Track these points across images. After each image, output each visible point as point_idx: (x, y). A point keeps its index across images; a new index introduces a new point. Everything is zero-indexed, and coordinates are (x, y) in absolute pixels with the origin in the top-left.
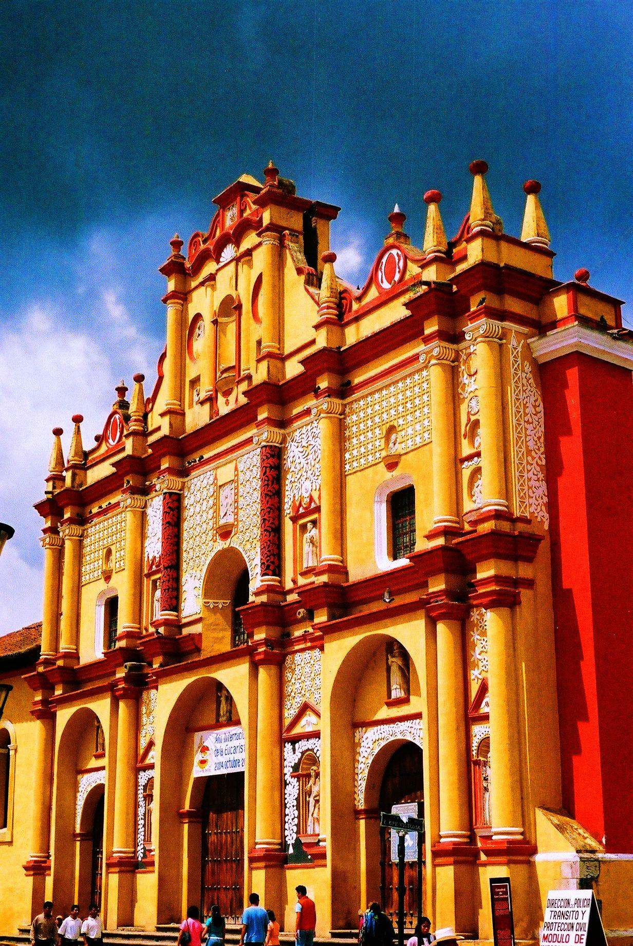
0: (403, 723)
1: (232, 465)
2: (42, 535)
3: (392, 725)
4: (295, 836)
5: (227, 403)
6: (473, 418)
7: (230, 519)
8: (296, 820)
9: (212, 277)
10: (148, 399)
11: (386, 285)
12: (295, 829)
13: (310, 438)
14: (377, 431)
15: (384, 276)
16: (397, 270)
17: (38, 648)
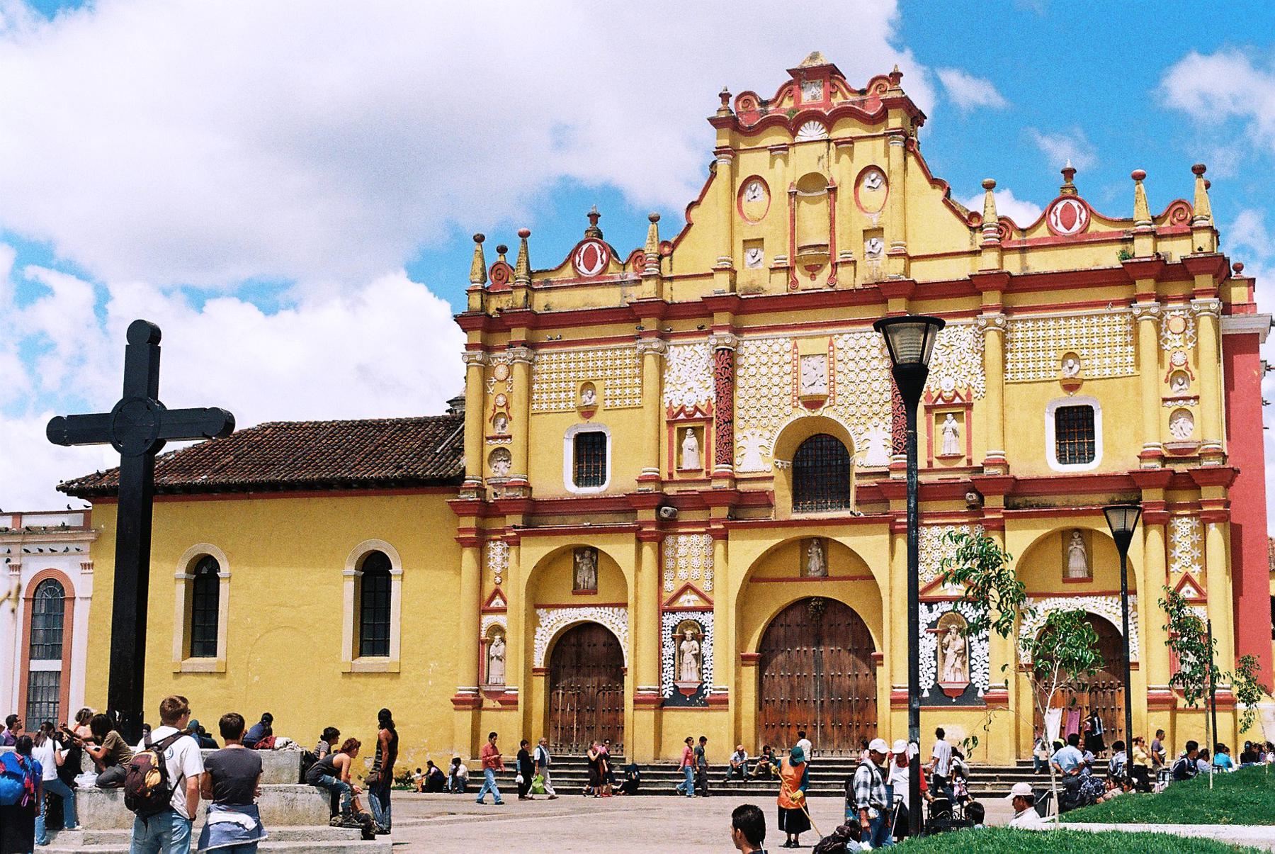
0: (1084, 598)
1: (827, 340)
2: (465, 351)
3: (1070, 599)
4: (932, 683)
5: (813, 277)
6: (1176, 369)
7: (824, 390)
8: (934, 670)
9: (785, 148)
10: (664, 243)
11: (1061, 228)
12: (933, 677)
13: (954, 339)
14: (1052, 353)
15: (1059, 220)
16: (1078, 220)
17: (464, 470)
